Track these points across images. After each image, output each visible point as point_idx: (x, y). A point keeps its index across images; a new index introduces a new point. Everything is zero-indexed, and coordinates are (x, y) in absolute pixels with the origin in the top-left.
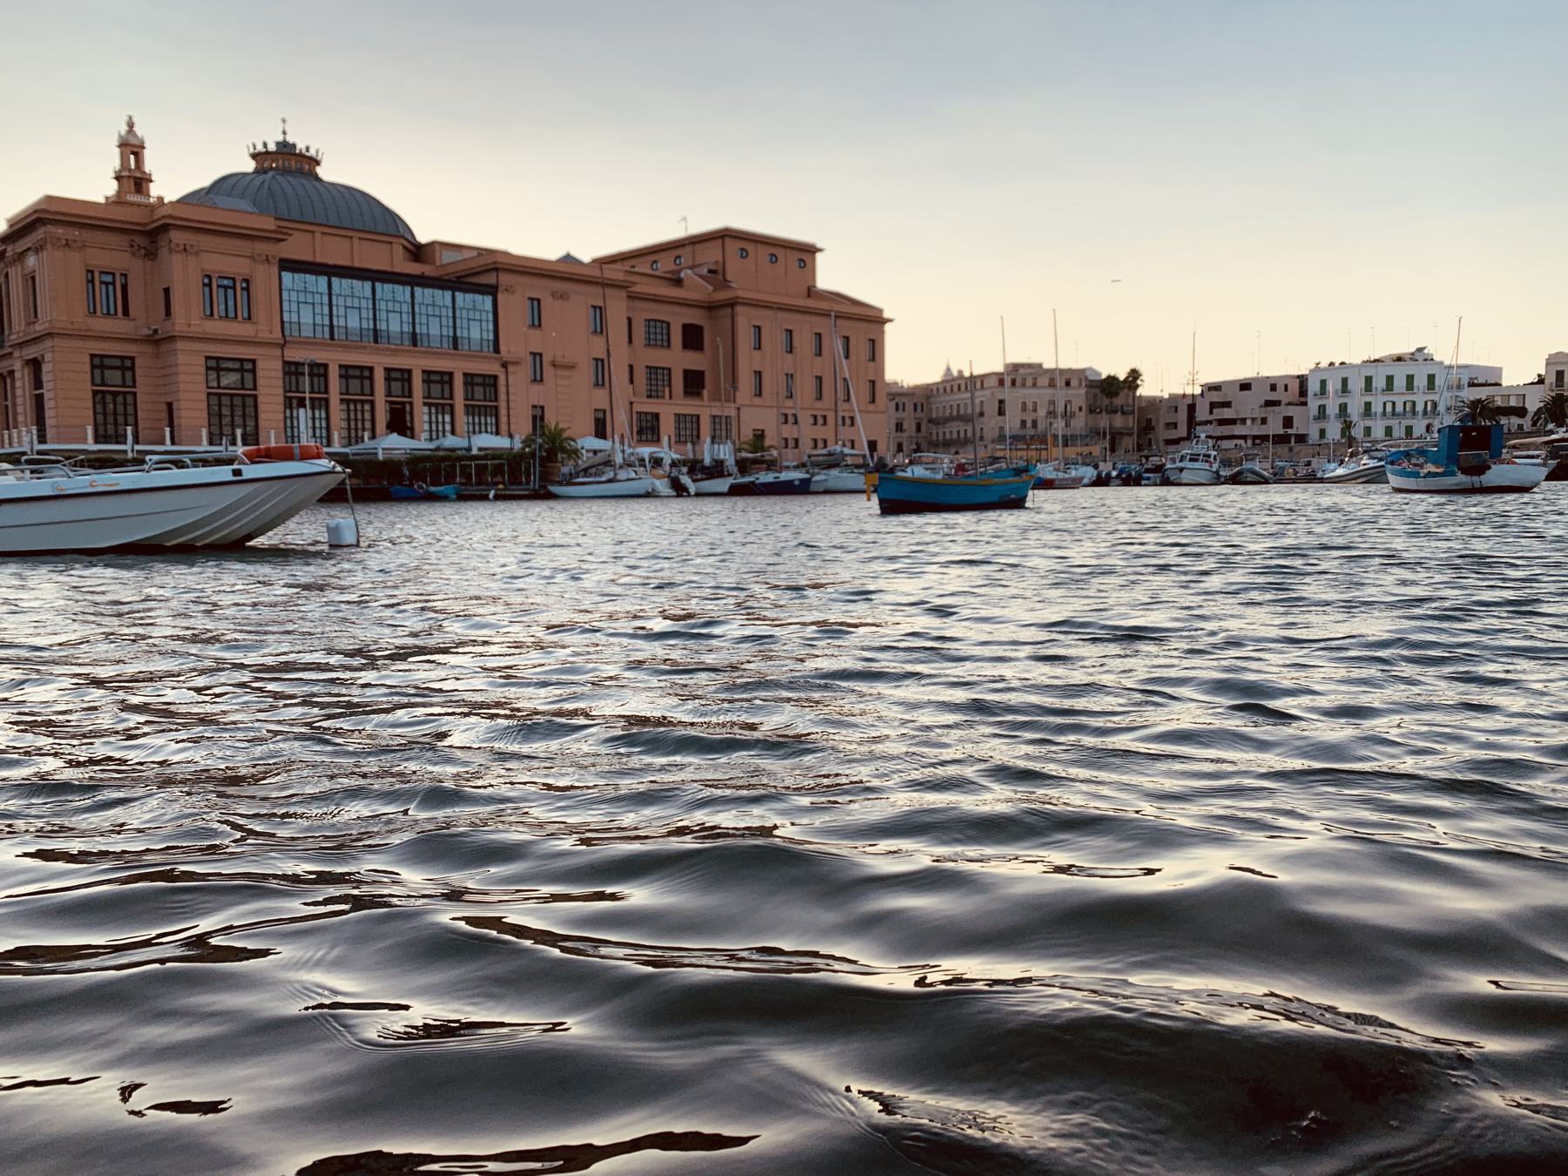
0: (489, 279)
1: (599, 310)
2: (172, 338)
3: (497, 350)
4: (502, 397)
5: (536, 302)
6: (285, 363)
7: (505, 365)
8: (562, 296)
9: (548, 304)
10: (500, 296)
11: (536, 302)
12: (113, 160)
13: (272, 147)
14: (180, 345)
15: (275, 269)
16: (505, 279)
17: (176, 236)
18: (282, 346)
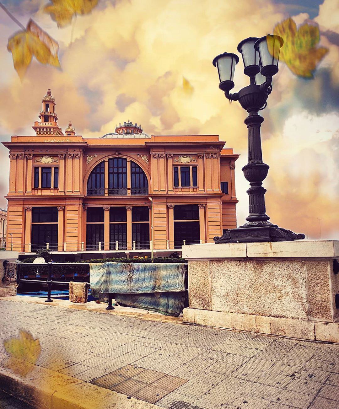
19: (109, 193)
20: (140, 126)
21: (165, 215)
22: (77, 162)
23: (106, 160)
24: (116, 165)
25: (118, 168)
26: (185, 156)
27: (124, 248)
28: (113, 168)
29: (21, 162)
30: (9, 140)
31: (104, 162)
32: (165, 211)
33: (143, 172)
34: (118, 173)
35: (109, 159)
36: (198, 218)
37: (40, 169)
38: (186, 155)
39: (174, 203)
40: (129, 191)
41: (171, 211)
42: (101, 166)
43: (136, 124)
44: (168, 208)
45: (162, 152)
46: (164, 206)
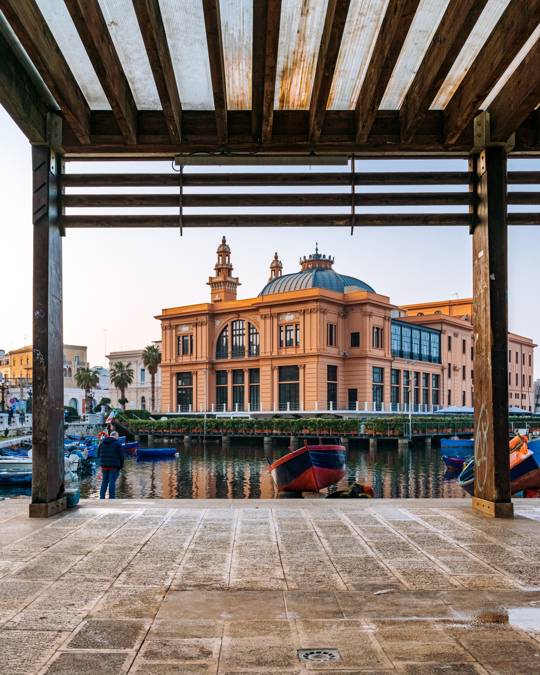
0: (438, 327)
1: (464, 341)
2: (365, 358)
3: (440, 362)
4: (442, 386)
5: (450, 338)
6: (392, 370)
7: (442, 370)
8: (456, 335)
9: (453, 339)
10: (442, 335)
11: (450, 338)
12: (214, 259)
13: (308, 258)
14: (368, 361)
15: (390, 323)
16: (445, 327)
17: (369, 309)
18: (391, 362)
19: (232, 356)
20: (330, 257)
21: (269, 377)
22: (204, 328)
23: (229, 323)
24: (238, 328)
25: (239, 330)
26: (289, 314)
27: (255, 409)
28: (236, 330)
29: (168, 332)
30: (160, 313)
31: (227, 326)
32: (269, 373)
33: (258, 333)
34: (239, 335)
35: (232, 323)
36: (297, 378)
37: (181, 339)
38: (289, 312)
39: (278, 363)
40: (246, 354)
41: (276, 373)
42: (225, 329)
43: (324, 256)
44: (272, 370)
45: (267, 311)
46: (269, 368)
